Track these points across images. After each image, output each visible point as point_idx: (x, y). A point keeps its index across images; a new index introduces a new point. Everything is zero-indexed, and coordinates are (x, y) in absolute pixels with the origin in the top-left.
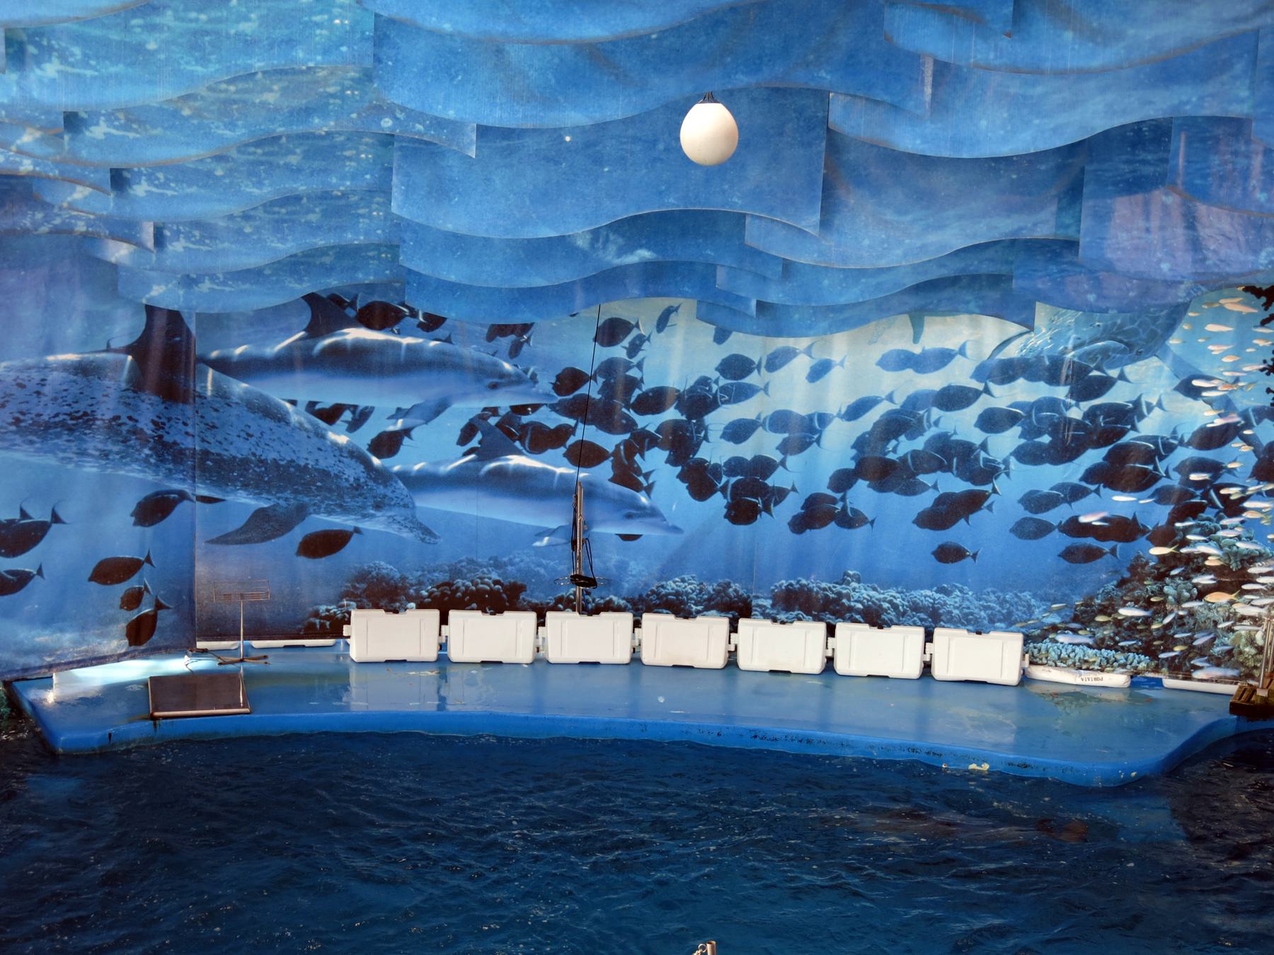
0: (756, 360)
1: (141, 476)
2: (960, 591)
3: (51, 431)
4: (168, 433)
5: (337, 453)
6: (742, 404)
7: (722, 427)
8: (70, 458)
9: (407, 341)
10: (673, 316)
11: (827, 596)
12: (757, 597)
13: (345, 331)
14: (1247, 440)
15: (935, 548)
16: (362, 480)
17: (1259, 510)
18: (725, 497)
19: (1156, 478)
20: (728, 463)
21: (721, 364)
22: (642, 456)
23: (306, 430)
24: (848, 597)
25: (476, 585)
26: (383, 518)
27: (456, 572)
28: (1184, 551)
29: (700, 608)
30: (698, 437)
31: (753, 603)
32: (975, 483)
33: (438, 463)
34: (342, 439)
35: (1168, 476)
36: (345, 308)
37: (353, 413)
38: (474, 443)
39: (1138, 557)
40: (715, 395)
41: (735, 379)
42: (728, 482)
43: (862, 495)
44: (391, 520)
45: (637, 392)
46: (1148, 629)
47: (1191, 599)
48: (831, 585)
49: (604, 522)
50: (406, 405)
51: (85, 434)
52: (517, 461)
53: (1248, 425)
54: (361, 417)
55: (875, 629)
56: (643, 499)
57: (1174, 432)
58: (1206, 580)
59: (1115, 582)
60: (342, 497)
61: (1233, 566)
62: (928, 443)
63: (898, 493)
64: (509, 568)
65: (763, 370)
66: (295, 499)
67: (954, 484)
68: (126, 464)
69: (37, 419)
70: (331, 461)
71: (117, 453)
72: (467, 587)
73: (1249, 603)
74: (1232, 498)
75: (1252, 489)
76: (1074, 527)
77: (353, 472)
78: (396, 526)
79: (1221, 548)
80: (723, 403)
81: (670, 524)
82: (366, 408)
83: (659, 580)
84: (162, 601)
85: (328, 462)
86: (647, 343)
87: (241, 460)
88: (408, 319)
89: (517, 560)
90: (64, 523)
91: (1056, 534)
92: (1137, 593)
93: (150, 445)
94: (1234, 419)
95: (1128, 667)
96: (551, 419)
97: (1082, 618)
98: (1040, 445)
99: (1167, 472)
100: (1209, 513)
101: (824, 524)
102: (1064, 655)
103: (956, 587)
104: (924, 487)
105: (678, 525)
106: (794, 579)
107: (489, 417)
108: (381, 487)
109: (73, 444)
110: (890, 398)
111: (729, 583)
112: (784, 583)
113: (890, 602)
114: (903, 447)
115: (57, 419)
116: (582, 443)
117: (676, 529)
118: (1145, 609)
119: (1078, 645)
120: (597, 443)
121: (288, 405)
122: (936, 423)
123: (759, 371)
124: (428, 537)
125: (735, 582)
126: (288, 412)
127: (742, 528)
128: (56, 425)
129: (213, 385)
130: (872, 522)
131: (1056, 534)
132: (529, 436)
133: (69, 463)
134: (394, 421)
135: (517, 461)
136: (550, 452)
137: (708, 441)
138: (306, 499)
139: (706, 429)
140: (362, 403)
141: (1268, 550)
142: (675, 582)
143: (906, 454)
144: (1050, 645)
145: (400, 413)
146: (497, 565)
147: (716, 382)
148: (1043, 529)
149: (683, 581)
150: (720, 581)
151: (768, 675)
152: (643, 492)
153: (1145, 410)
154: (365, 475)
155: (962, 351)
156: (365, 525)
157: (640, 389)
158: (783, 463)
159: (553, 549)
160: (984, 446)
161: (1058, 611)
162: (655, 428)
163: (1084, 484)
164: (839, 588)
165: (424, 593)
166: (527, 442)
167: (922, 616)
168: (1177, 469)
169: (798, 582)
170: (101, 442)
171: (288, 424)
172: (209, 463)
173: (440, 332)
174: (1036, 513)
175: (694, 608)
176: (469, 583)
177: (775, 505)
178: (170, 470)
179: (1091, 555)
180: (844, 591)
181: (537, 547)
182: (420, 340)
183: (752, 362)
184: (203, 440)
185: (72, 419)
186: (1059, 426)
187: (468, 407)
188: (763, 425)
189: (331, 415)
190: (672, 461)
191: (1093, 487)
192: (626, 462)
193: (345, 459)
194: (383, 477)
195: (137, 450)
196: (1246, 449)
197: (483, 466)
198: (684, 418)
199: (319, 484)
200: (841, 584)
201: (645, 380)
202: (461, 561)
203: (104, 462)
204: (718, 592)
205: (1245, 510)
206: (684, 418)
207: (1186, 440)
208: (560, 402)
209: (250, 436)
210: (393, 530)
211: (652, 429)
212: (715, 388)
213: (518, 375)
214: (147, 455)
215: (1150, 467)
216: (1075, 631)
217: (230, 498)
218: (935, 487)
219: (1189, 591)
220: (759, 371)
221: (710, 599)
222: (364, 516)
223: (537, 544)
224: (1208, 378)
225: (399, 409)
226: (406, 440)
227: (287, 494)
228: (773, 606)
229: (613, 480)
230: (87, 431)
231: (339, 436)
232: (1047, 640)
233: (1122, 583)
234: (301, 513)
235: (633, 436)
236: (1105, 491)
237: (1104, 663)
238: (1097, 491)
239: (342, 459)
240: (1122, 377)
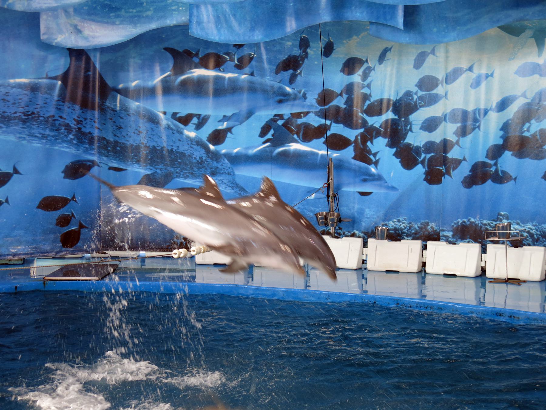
1: (67, 150)
3: (12, 122)
4: (85, 127)
5: (189, 143)
6: (432, 107)
7: (421, 122)
8: (24, 138)
9: (228, 75)
10: (388, 53)
11: (487, 229)
12: (444, 231)
13: (193, 71)
16: (204, 158)
18: (424, 167)
20: (425, 145)
21: (418, 82)
22: (372, 143)
23: (172, 129)
30: (406, 130)
31: (441, 234)
33: (248, 148)
36: (192, 57)
37: (198, 118)
38: (269, 136)
40: (416, 102)
41: (428, 91)
42: (425, 157)
44: (221, 182)
45: (368, 103)
48: (489, 222)
49: (349, 184)
50: (229, 114)
51: (34, 125)
52: (296, 147)
54: (202, 122)
55: (519, 249)
56: (373, 170)
60: (193, 168)
63: (531, 158)
66: (165, 169)
68: (59, 143)
69: (3, 114)
70: (186, 147)
71: (53, 136)
77: (198, 153)
80: (421, 107)
81: (390, 185)
82: (206, 116)
83: (384, 221)
84: (84, 224)
85: (184, 148)
86: (373, 71)
87: (136, 146)
88: (229, 62)
90: (21, 174)
93: (73, 133)
96: (315, 121)
101: (484, 181)
105: (395, 186)
106: (466, 218)
107: (278, 120)
108: (215, 162)
109: (26, 130)
110: (524, 95)
111: (428, 223)
112: (460, 221)
115: (15, 115)
116: (334, 135)
117: (393, 188)
120: (344, 135)
123: (442, 85)
124: (242, 193)
125: (431, 222)
127: (435, 187)
128: (15, 118)
129: (120, 104)
130: (515, 179)
132: (302, 132)
133: (23, 140)
134: (222, 123)
135: (296, 147)
136: (315, 141)
137: (412, 132)
139: (410, 124)
140: (203, 113)
142: (394, 222)
147: (416, 94)
149: (399, 221)
150: (422, 221)
151: (442, 277)
152: (373, 165)
154: (205, 155)
157: (370, 101)
158: (457, 143)
159: (317, 201)
162: (379, 125)
166: (301, 135)
169: (469, 220)
170: (43, 129)
172: (118, 148)
173: (247, 70)
177: (453, 171)
178: (87, 148)
182: (236, 75)
184: (115, 136)
185: (24, 115)
189: (185, 120)
190: (391, 145)
192: (362, 147)
193: (195, 147)
194: (216, 156)
195: (65, 136)
197: (275, 150)
198: (396, 117)
199: (179, 161)
200: (496, 221)
201: (372, 95)
203: (44, 141)
206: (396, 117)
208: (320, 111)
211: (377, 125)
212: (415, 97)
213: (295, 95)
214: (71, 139)
217: (129, 168)
220: (442, 85)
221: (416, 234)
225: (225, 116)
226: (229, 135)
227: (160, 167)
228: (453, 236)
229: (355, 158)
230: (35, 123)
231: (190, 133)
235: (366, 130)
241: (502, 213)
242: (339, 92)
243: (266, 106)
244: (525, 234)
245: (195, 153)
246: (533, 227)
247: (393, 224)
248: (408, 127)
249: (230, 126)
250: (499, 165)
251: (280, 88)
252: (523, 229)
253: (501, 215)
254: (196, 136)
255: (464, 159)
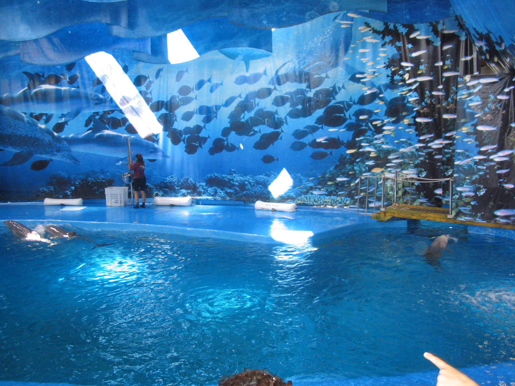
0: (192, 88)
2: (274, 175)
10: (161, 73)
13: (41, 86)
14: (382, 99)
15: (262, 157)
16: (51, 141)
17: (389, 130)
18: (184, 143)
19: (345, 120)
20: (185, 129)
23: (30, 123)
24: (233, 180)
25: (95, 179)
26: (60, 155)
27: (88, 175)
28: (361, 150)
29: (179, 188)
32: (275, 129)
33: (78, 134)
34: (43, 126)
35: (350, 118)
36: (40, 77)
37: (46, 116)
38: (91, 126)
39: (342, 155)
42: (185, 137)
43: (233, 137)
46: (349, 186)
47: (365, 172)
50: (65, 112)
53: (381, 93)
57: (351, 99)
58: (371, 163)
59: (333, 167)
61: (382, 156)
62: (256, 113)
64: (108, 173)
65: (194, 90)
67: (266, 129)
72: (92, 181)
73: (390, 172)
74: (378, 125)
75: (386, 121)
76: (315, 144)
77: (48, 138)
78: (65, 158)
79: (376, 148)
80: (181, 105)
82: (51, 114)
85: (39, 135)
89: (110, 170)
91: (308, 147)
92: (343, 171)
94: (375, 90)
95: (342, 203)
97: (321, 183)
98: (298, 110)
99: (350, 116)
100: (369, 133)
102: (316, 199)
103: (272, 173)
104: (256, 132)
108: (58, 144)
110: (240, 96)
113: (248, 181)
114: (246, 116)
118: (347, 177)
119: (322, 195)
121: (23, 115)
122: (258, 104)
123: (193, 92)
126: (23, 117)
131: (308, 147)
134: (61, 119)
135: (107, 132)
136: (120, 128)
137: (177, 121)
138: (32, 149)
139: (176, 116)
140: (49, 112)
141: (395, 148)
143: (248, 119)
144: (310, 195)
145: (63, 116)
146: (103, 172)
147: (178, 97)
148: (302, 146)
149: (172, 177)
152: (156, 143)
153: (338, 90)
155: (265, 73)
156: (54, 158)
158: (204, 127)
160: (276, 112)
161: (312, 181)
163: (316, 125)
164: (229, 177)
165: (77, 183)
167: (261, 186)
168: (354, 115)
171: (24, 121)
174: (299, 139)
175: (177, 188)
176: (93, 179)
179: (322, 156)
180: (231, 178)
181: (117, 165)
183: (190, 88)
186: (306, 101)
187: (87, 113)
188: (196, 113)
189: (38, 118)
191: (320, 126)
193: (45, 134)
194: (58, 140)
196: (381, 103)
199: (36, 143)
201: (153, 98)
202: (89, 171)
204: (184, 182)
205: (384, 130)
206: (168, 112)
207: (356, 102)
209: (11, 126)
210: (64, 160)
212: (178, 99)
215: (342, 115)
216: (320, 189)
217: (6, 149)
218: (260, 131)
219: (364, 168)
221: (182, 185)
222: (53, 155)
223: (117, 164)
224: (362, 73)
225: (63, 115)
226: (66, 126)
232: (309, 194)
233: (336, 167)
234: (30, 154)
236: (325, 127)
237: (333, 202)
238: (322, 128)
239: (44, 134)
240: (327, 77)
241: (233, 170)
242: (133, 98)
243: (89, 107)
244: (247, 183)
245: (45, 138)
246: (251, 178)
247: (169, 179)
248: (175, 118)
249: (67, 120)
250: (229, 140)
251: (96, 95)
252: (245, 179)
253: (232, 171)
254: (45, 127)
255: (209, 137)
